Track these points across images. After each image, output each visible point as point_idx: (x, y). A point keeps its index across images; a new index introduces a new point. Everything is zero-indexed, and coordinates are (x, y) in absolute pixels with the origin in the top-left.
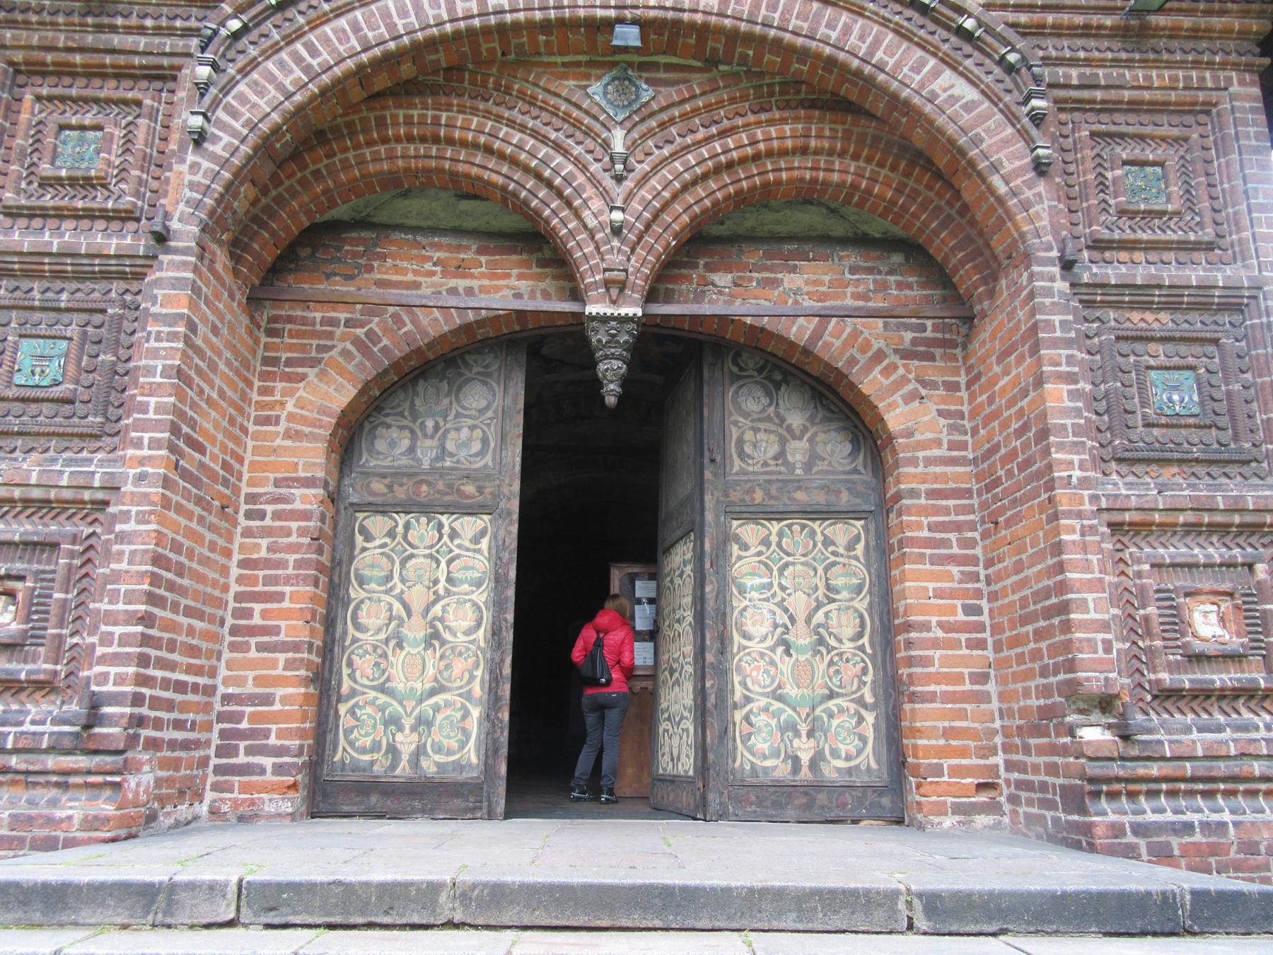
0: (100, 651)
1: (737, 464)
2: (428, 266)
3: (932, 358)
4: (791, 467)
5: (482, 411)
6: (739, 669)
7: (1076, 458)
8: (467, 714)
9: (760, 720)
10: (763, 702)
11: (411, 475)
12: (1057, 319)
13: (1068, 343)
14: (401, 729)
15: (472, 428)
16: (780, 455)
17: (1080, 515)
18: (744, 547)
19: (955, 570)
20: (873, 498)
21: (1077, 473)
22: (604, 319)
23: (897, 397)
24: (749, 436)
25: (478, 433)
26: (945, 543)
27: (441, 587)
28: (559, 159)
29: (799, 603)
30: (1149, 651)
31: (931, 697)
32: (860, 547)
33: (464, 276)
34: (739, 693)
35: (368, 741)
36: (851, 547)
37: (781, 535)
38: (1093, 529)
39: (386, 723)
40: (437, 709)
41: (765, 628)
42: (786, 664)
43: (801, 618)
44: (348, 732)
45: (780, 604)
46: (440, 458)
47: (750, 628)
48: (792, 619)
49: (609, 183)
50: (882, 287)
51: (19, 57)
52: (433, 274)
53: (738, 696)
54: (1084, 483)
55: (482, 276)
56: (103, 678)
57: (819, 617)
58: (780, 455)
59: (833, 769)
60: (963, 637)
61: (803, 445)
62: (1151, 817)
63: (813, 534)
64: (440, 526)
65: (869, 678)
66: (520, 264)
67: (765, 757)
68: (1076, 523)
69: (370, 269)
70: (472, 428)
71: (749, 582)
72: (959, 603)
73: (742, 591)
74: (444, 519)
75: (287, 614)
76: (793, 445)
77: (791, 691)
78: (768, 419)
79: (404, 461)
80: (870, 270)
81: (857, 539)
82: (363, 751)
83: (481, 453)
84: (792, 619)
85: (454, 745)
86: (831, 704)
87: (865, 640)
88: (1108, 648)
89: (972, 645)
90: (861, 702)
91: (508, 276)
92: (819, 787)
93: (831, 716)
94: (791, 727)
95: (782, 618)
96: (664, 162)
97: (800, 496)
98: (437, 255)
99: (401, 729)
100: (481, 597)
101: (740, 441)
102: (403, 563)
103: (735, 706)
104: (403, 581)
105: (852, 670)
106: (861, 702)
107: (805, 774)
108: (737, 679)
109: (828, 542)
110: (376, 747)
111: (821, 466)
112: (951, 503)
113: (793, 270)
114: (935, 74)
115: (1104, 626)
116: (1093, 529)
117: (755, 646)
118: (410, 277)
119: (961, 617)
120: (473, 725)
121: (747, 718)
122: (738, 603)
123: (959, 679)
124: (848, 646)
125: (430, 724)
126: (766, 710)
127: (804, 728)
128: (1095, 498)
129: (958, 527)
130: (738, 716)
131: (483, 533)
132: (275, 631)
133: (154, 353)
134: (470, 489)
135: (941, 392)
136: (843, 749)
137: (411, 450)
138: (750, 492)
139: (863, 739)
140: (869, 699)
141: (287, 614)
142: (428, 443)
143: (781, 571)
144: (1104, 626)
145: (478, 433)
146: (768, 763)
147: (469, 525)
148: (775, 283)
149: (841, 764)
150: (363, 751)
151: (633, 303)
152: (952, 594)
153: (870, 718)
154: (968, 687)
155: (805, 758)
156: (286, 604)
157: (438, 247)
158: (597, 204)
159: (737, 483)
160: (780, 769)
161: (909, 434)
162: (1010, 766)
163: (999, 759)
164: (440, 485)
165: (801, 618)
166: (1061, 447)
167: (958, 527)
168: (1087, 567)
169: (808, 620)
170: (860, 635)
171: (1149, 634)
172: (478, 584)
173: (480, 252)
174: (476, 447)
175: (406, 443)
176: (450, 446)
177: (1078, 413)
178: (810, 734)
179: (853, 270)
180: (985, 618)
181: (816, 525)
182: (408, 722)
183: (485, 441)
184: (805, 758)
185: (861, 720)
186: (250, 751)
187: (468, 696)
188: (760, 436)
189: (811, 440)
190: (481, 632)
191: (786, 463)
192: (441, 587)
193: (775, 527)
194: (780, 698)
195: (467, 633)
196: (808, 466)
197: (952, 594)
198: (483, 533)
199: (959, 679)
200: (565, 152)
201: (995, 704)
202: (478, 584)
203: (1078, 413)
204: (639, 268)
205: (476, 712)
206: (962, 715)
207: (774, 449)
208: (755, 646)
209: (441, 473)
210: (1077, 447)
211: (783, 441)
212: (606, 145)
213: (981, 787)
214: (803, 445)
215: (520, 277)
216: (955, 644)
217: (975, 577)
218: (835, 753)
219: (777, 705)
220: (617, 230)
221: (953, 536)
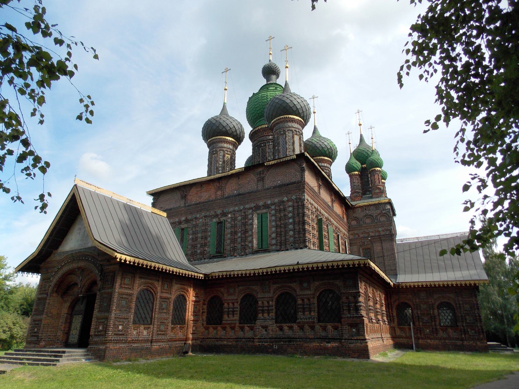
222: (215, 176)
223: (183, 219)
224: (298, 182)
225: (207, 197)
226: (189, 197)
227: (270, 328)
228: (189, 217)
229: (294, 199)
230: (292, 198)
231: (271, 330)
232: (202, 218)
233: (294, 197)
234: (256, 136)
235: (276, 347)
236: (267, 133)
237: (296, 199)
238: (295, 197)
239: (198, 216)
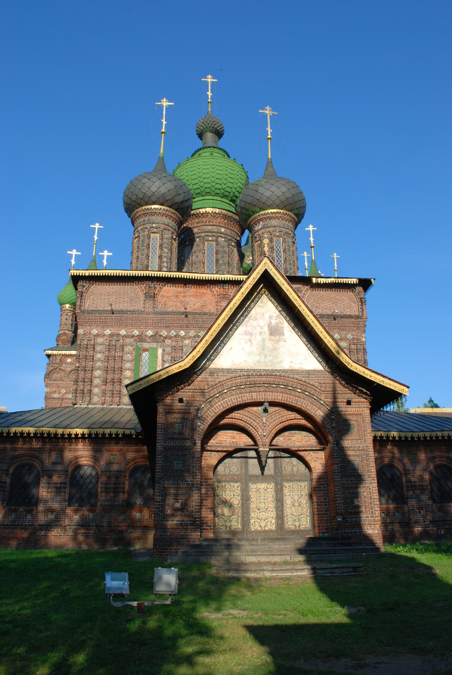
0: (194, 511)
1: (284, 471)
2: (228, 437)
3: (319, 453)
4: (294, 472)
5: (237, 463)
6: (286, 510)
7: (338, 477)
8: (238, 519)
9: (289, 519)
10: (290, 516)
11: (225, 475)
12: (335, 454)
13: (337, 458)
14: (227, 522)
15: (235, 466)
16: (292, 470)
17: (338, 486)
18: (286, 487)
19: (322, 492)
20: (309, 478)
21: (338, 480)
22: (262, 451)
23: (312, 461)
24: (286, 466)
25: (236, 467)
26: (321, 487)
27: (232, 496)
28: (254, 422)
29: (296, 498)
30: (348, 507)
32: (307, 487)
33: (235, 439)
34: (286, 514)
35: (221, 525)
36: (305, 487)
37: (292, 485)
38: (340, 488)
39: (224, 521)
40: (233, 519)
41: (290, 503)
42: (294, 509)
43: (296, 501)
44: (218, 523)
45: (293, 498)
46: (230, 472)
47: (287, 502)
48: (295, 501)
49: (263, 427)
50: (310, 440)
51: (167, 411)
52: (229, 438)
53: (285, 515)
54: (339, 481)
55: (238, 439)
56: (196, 515)
57: (299, 500)
58: (292, 470)
59: (302, 527)
60: (323, 504)
61: (296, 468)
62: (347, 531)
63: (298, 485)
64: (231, 485)
65: (308, 511)
66: (244, 436)
68: (338, 487)
69: (217, 438)
70: (235, 466)
71: (287, 494)
72: (323, 498)
73: (286, 495)
74: (231, 484)
75: (209, 503)
76: (294, 468)
77: (295, 514)
78: (290, 463)
79: (223, 473)
80: (308, 436)
81: (306, 486)
82: (220, 526)
83: (237, 471)
84: (295, 501)
85: (236, 525)
86: (302, 516)
87: (308, 504)
88: (341, 506)
89: (325, 505)
90: (307, 515)
91: (242, 439)
92: (300, 531)
93: (302, 518)
94: (294, 520)
95: (293, 501)
96: (272, 422)
97: (296, 478)
98: (229, 435)
99: (227, 522)
100: (239, 498)
101: (285, 467)
102: (225, 492)
103: (285, 517)
104: (225, 495)
105: (305, 510)
106: (307, 515)
107: (297, 528)
108: (285, 512)
109: (301, 486)
110: (223, 525)
111: (299, 472)
112: (322, 480)
113: (294, 436)
114: (317, 410)
115: (341, 503)
116: (340, 488)
117: (288, 506)
118: (225, 439)
119: (323, 500)
120: (240, 521)
121: (287, 519)
122: (285, 498)
123: (322, 511)
124: (305, 505)
125: (232, 521)
126: (290, 517)
127: (297, 520)
128: (340, 483)
129: (322, 484)
130: (285, 518)
131: (239, 486)
132: (208, 506)
133: (196, 463)
134: (236, 478)
135: (320, 460)
136: (304, 524)
137: (225, 470)
138: (287, 477)
139: (307, 522)
140: (308, 515)
141: (209, 503)
142: (228, 469)
143: (293, 492)
144: (341, 503)
145: (236, 467)
146: (291, 527)
147: (236, 485)
148: (290, 439)
149: (304, 526)
150: (220, 526)
151: (267, 448)
152: (322, 496)
153: (308, 518)
154: (324, 512)
155: (297, 525)
156: (209, 501)
157: (229, 433)
158: (261, 430)
159: (284, 475)
160: (293, 528)
161: (314, 468)
162: (331, 525)
163: (329, 524)
164: (230, 477)
165: (296, 501)
166: (335, 475)
167: (322, 484)
168: (339, 494)
169: (298, 501)
170: (307, 503)
171: (348, 504)
172: (238, 496)
173: (237, 434)
174: (236, 470)
175: (223, 469)
176: (232, 470)
177: (338, 470)
178: (298, 521)
179: (305, 436)
180: (327, 500)
181: (299, 483)
182: (228, 521)
183: (238, 469)
184: (297, 525)
185: (307, 518)
186: (206, 526)
187: (238, 516)
188: (288, 466)
189: (298, 467)
190: (240, 505)
191: (293, 471)
192: (232, 496)
193: (291, 484)
194: (293, 515)
195: (237, 505)
196: (297, 472)
197: (322, 496)
198: (239, 486)
199: (322, 511)
200: (255, 421)
201: (328, 515)
202: (238, 496)
203: (338, 470)
204: (268, 441)
205: (240, 519)
206: (323, 517)
207: (291, 469)
208: (288, 506)
209: (231, 475)
210: (338, 475)
211: (292, 467)
212: (262, 420)
213: (326, 529)
214: (296, 468)
215: (245, 439)
216: (322, 505)
217: (325, 493)
218: (302, 524)
219: (292, 516)
220: (264, 436)
221: (322, 486)
222: (223, 276)
223: (150, 333)
224: (358, 317)
225: (198, 305)
226: (159, 298)
227: (430, 509)
228: (164, 333)
229: (350, 339)
230: (348, 337)
231: (432, 511)
232: (189, 338)
233: (350, 336)
234: (197, 220)
235: (441, 531)
236: (218, 222)
237: (353, 339)
238: (352, 337)
239: (182, 333)
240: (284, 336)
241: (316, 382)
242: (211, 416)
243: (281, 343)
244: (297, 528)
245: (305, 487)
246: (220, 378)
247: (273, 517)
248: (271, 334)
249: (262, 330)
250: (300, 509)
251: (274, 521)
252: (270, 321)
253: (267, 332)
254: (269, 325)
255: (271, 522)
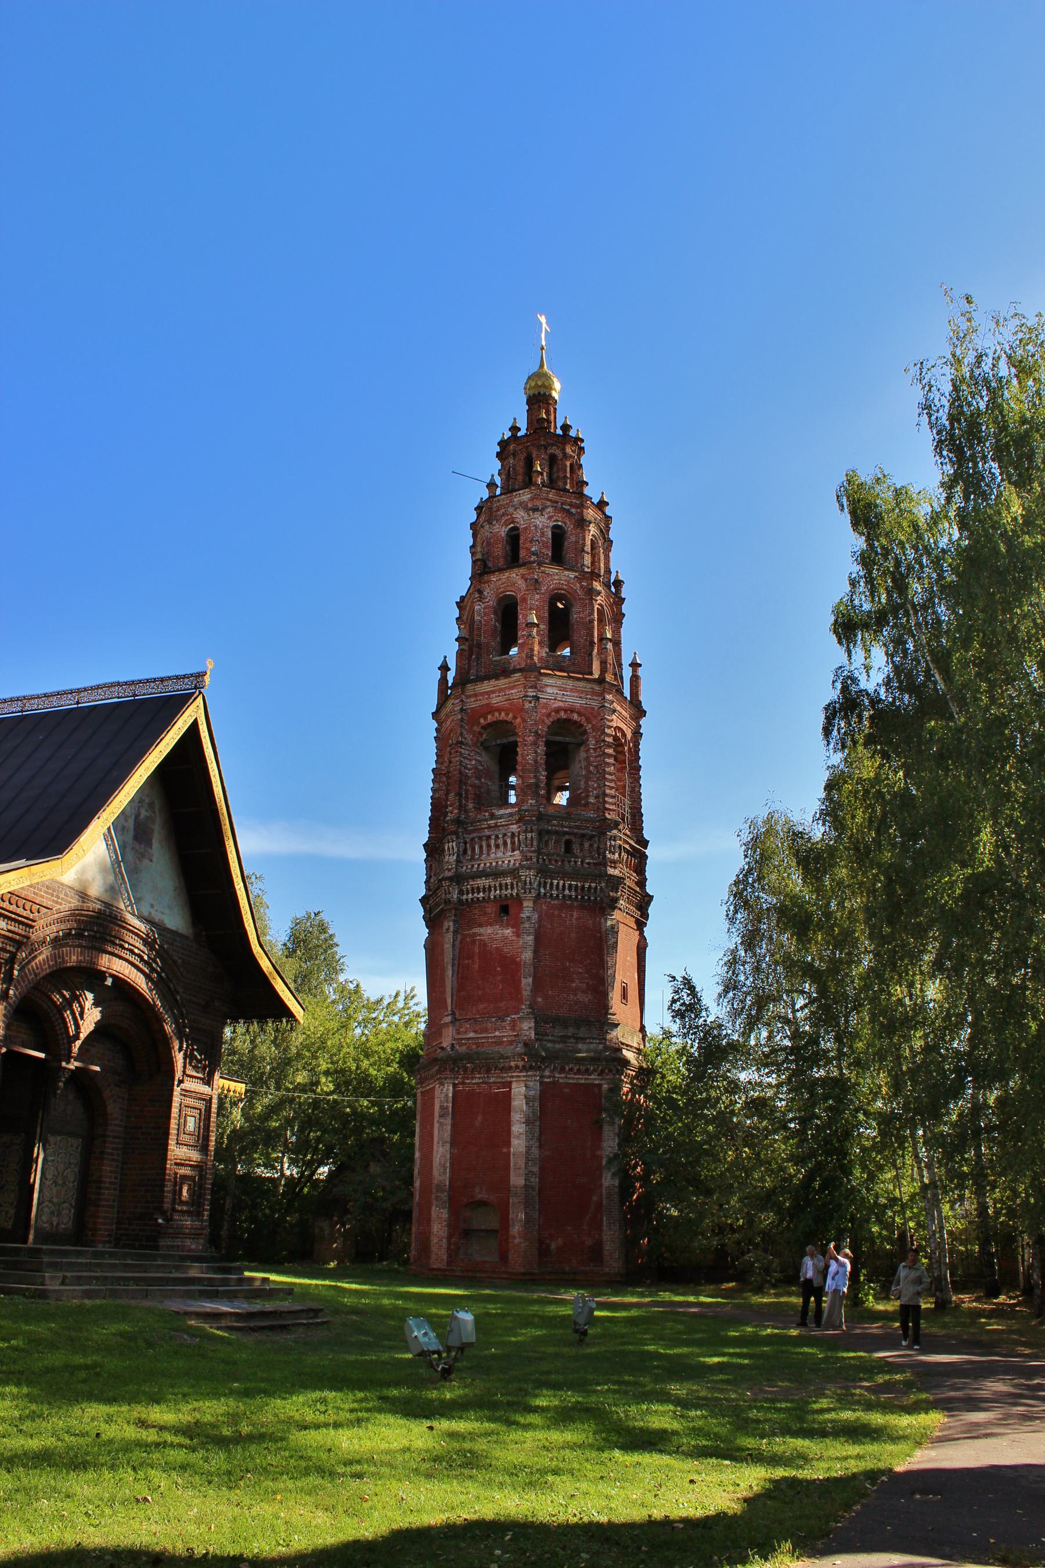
10: (47, 1203)
29: (61, 1167)
31: (103, 1206)
32: (80, 1148)
67: (44, 1223)
77: (55, 1200)
95: (56, 1174)
106: (71, 1205)
126: (47, 1206)
127: (56, 1213)
139: (70, 1217)
140: (74, 1204)
149: (63, 1226)
153: (73, 1211)
155: (55, 1223)
184: (55, 1223)
193: (59, 1138)
219: (50, 1205)
240: (151, 849)
241: (179, 958)
242: (28, 980)
243: (146, 862)
244: (54, 1228)
245: (77, 1149)
246: (61, 904)
247: (12, 1204)
248: (136, 838)
249: (125, 824)
250: (63, 1192)
251: (12, 1212)
252: (139, 809)
253: (131, 833)
254: (137, 816)
255: (7, 1212)
